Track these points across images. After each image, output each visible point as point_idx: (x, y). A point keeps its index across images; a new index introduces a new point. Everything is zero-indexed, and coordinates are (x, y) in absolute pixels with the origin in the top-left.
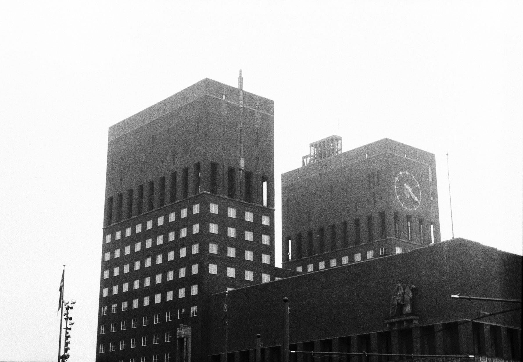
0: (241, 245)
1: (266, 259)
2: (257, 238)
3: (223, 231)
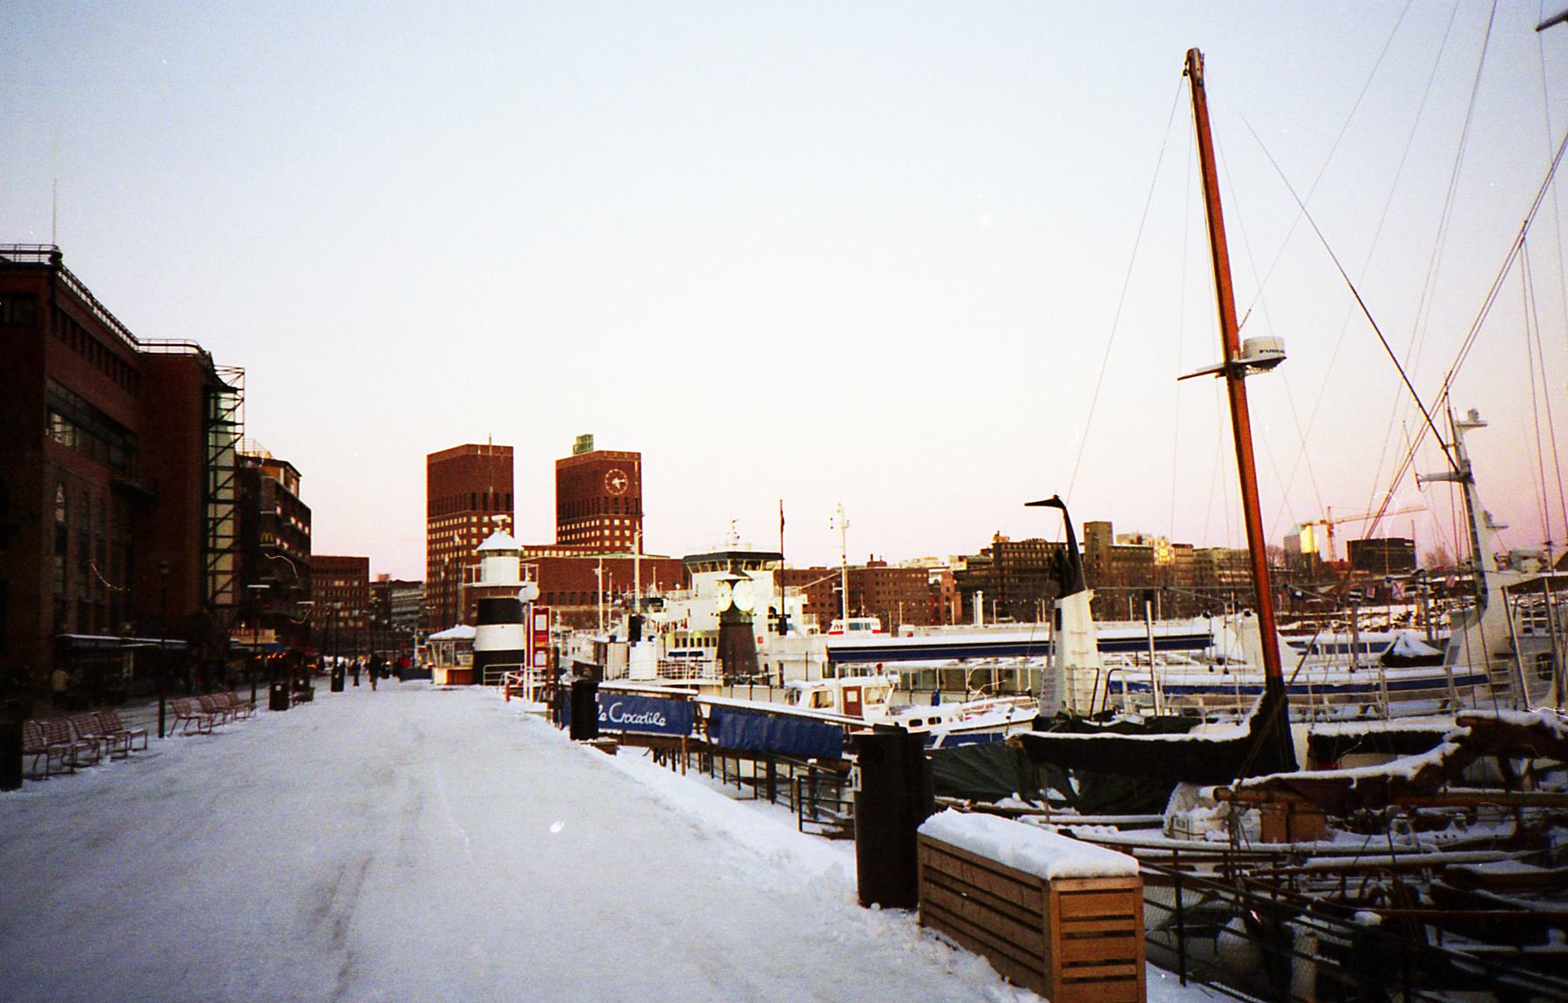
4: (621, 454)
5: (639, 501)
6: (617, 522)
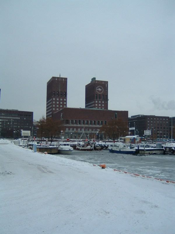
0: (59, 104)
1: (65, 106)
2: (63, 103)
3: (56, 103)
4: (102, 82)
5: (107, 96)
6: (100, 102)
